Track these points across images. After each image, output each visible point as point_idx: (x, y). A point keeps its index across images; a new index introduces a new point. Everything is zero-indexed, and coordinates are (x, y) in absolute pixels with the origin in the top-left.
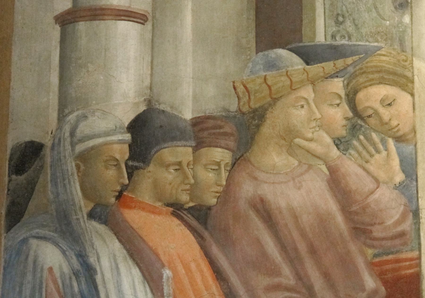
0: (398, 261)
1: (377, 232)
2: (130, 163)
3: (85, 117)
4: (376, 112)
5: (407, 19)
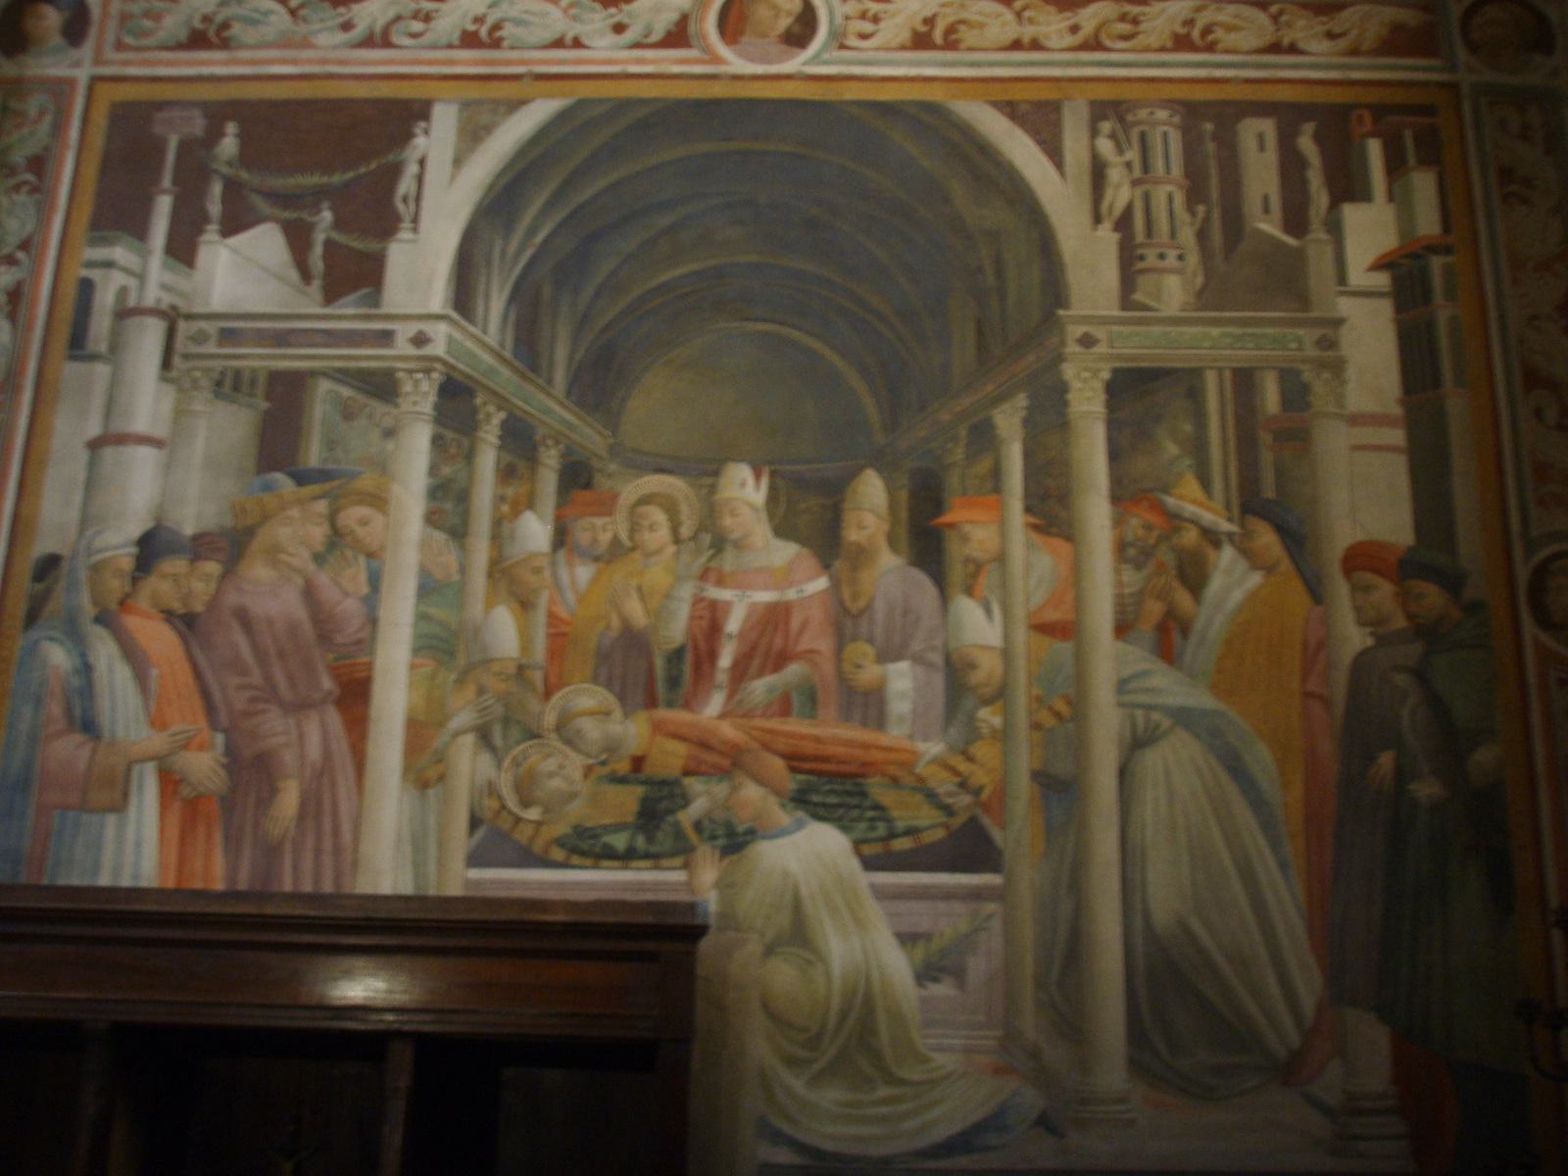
0: (355, 665)
1: (339, 639)
2: (136, 574)
3: (98, 533)
4: (352, 532)
5: (390, 446)
